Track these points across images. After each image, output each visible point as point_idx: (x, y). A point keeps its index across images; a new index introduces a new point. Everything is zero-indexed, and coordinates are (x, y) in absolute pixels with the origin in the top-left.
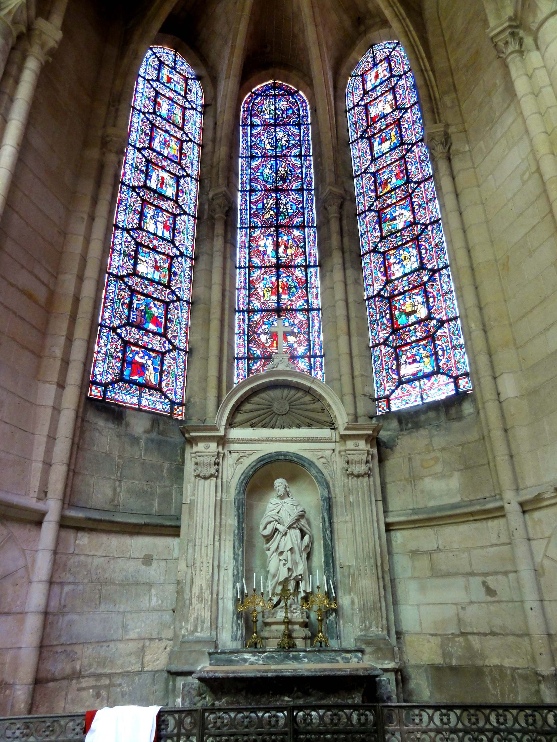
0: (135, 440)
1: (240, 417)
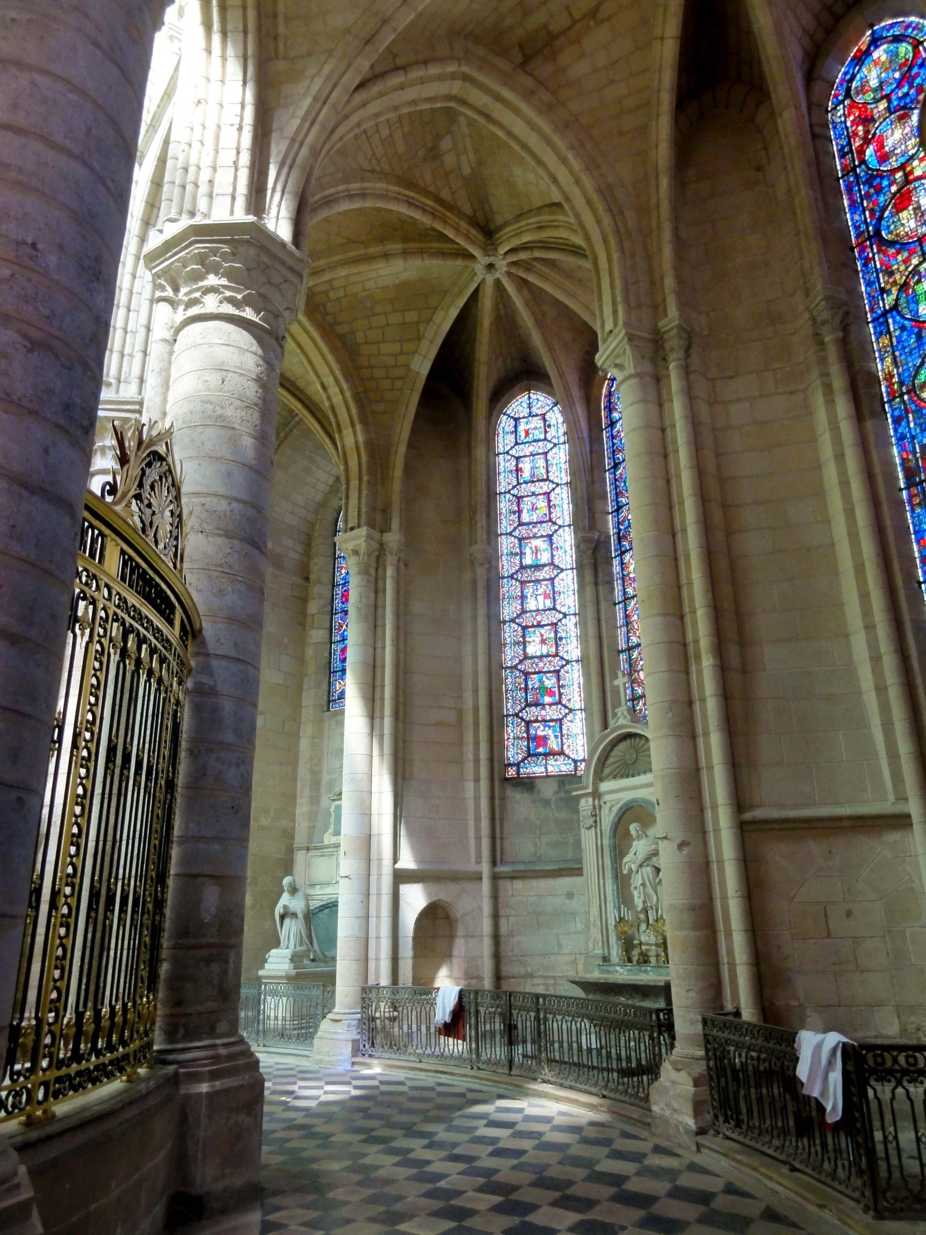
0: (547, 803)
1: (607, 771)
